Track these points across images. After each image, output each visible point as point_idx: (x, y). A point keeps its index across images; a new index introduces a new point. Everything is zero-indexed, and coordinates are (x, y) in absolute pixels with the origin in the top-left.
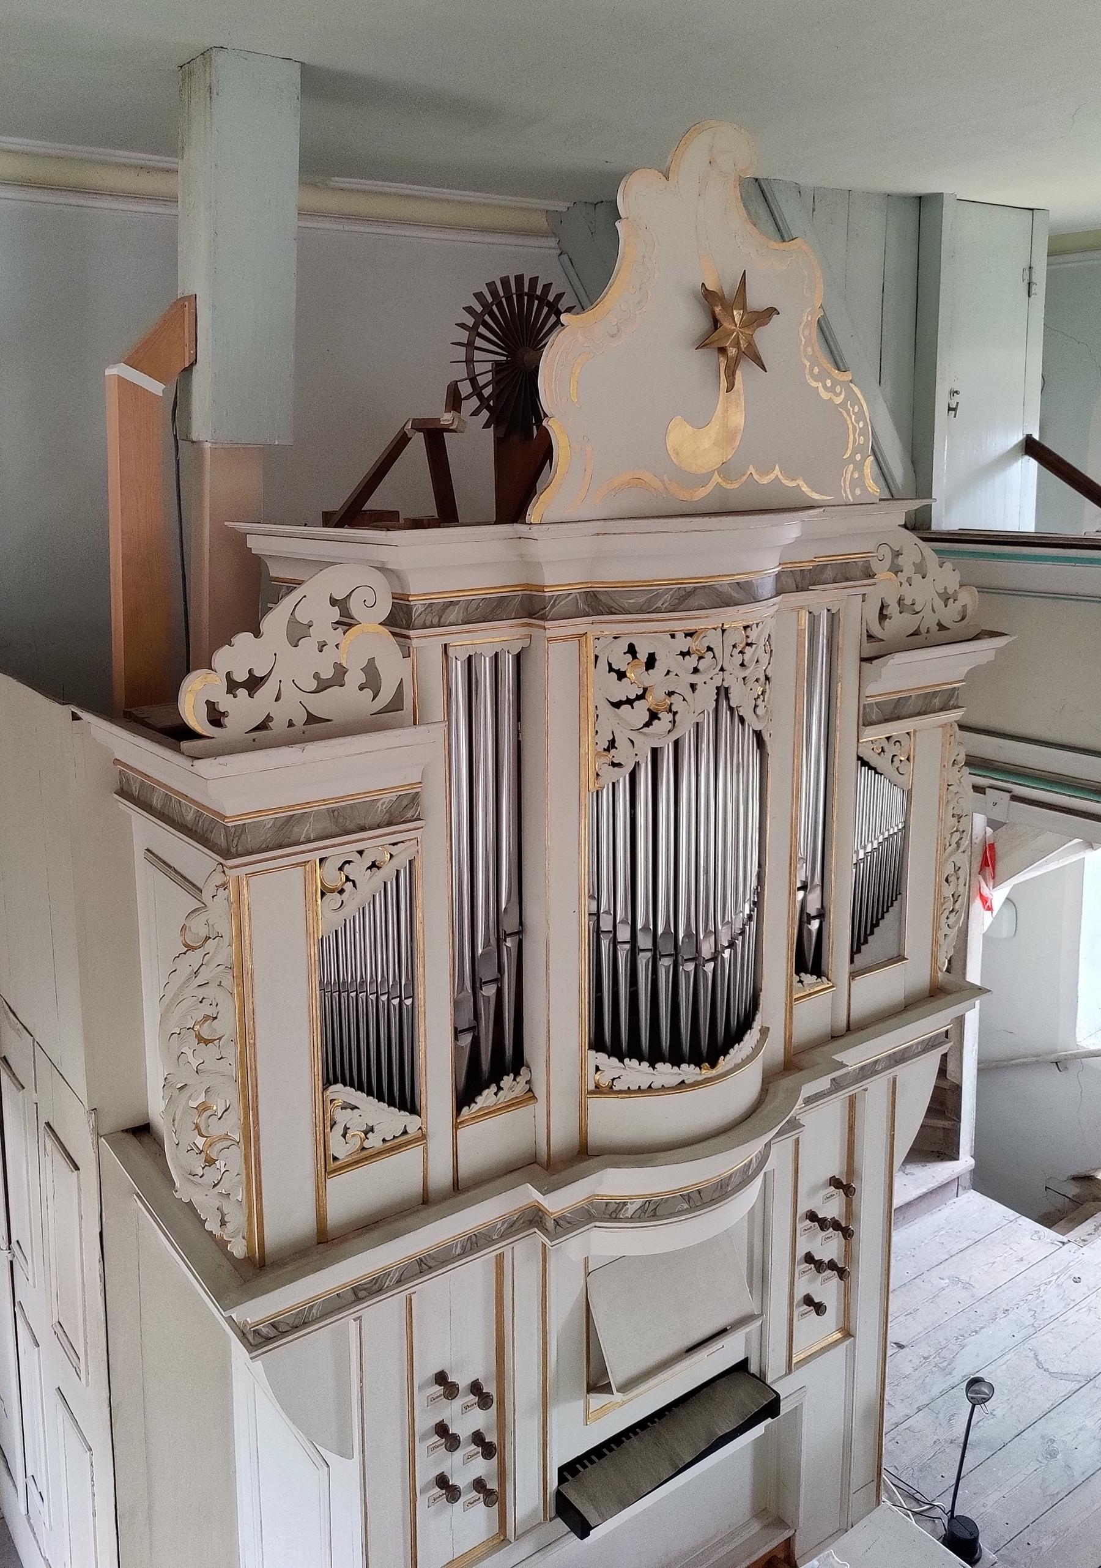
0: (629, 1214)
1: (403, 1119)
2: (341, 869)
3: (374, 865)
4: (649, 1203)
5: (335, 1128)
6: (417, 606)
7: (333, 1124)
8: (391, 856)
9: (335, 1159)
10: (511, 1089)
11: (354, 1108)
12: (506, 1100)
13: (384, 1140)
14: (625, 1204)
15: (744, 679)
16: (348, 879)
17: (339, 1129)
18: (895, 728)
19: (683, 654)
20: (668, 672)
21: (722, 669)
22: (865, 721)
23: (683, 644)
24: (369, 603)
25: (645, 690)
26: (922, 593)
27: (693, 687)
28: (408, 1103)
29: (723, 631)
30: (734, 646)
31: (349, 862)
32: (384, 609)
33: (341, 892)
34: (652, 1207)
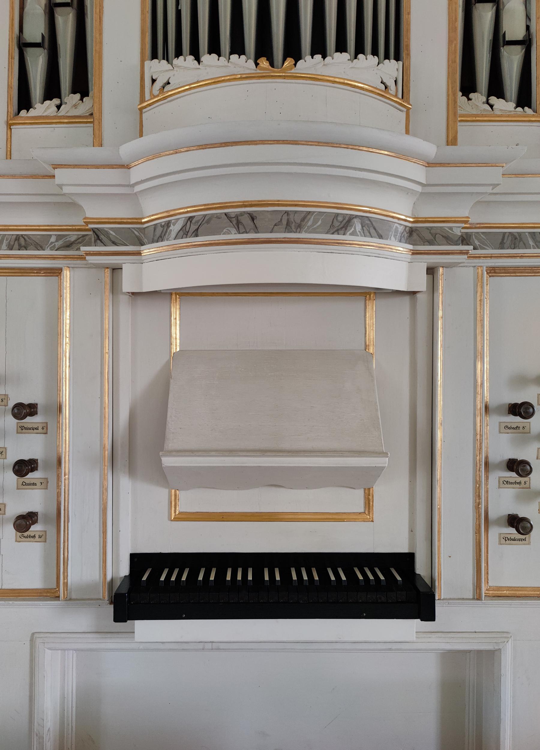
4: (191, 222)
10: (75, 106)
12: (67, 115)
14: (168, 224)
34: (193, 228)
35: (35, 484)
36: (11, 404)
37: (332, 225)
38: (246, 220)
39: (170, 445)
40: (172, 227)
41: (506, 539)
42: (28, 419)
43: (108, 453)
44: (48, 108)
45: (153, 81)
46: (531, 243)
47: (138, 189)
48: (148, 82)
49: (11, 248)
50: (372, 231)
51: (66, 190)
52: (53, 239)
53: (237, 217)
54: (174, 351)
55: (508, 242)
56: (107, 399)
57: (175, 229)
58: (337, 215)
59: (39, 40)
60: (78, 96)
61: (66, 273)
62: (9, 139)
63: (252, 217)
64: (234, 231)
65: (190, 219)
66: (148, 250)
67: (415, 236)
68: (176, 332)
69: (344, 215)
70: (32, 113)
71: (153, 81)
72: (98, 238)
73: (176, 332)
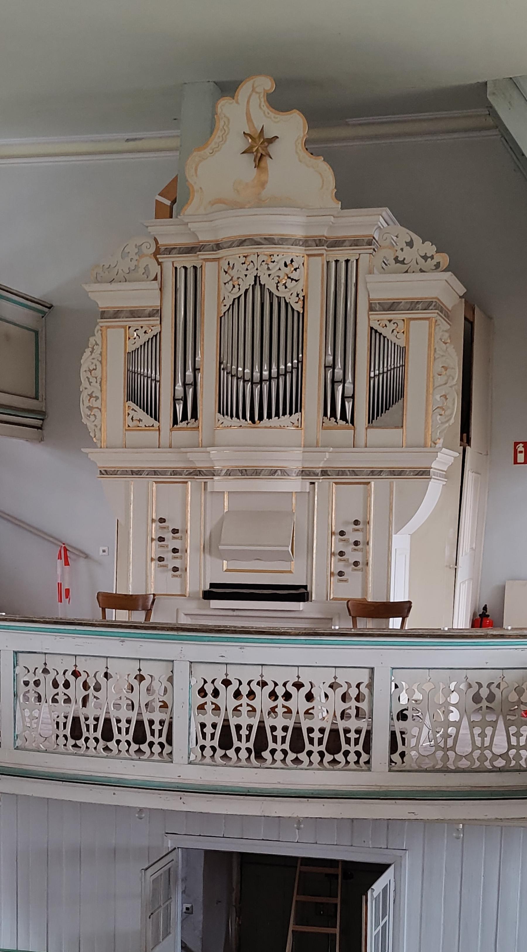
0: (223, 475)
1: (152, 421)
2: (135, 331)
3: (145, 332)
5: (129, 416)
6: (163, 248)
7: (129, 414)
8: (152, 330)
9: (129, 426)
10: (193, 424)
11: (135, 411)
13: (145, 426)
14: (222, 470)
15: (269, 275)
16: (137, 335)
17: (130, 416)
18: (397, 316)
19: (243, 264)
20: (238, 271)
21: (257, 269)
22: (371, 309)
23: (243, 260)
24: (148, 247)
25: (232, 278)
26: (408, 254)
27: (246, 275)
28: (156, 418)
29: (258, 256)
30: (263, 261)
31: (138, 330)
32: (153, 249)
33: (135, 339)
35: (177, 558)
36: (171, 529)
37: (270, 473)
38: (244, 471)
39: (222, 542)
40: (223, 471)
41: (340, 581)
42: (176, 535)
43: (202, 547)
44: (184, 424)
45: (219, 420)
46: (348, 473)
47: (213, 459)
48: (217, 420)
49: (171, 475)
50: (285, 474)
51: (190, 459)
52: (185, 471)
53: (242, 470)
54: (225, 511)
55: (340, 473)
56: (202, 528)
57: (224, 472)
58: (272, 470)
59: (181, 398)
60: (194, 420)
61: (189, 483)
62: (171, 435)
63: (246, 470)
64: (240, 475)
65: (228, 470)
66: (216, 478)
67: (304, 473)
68: (226, 504)
69: (274, 470)
70: (178, 426)
71: (219, 420)
72: (200, 473)
73: (226, 504)
